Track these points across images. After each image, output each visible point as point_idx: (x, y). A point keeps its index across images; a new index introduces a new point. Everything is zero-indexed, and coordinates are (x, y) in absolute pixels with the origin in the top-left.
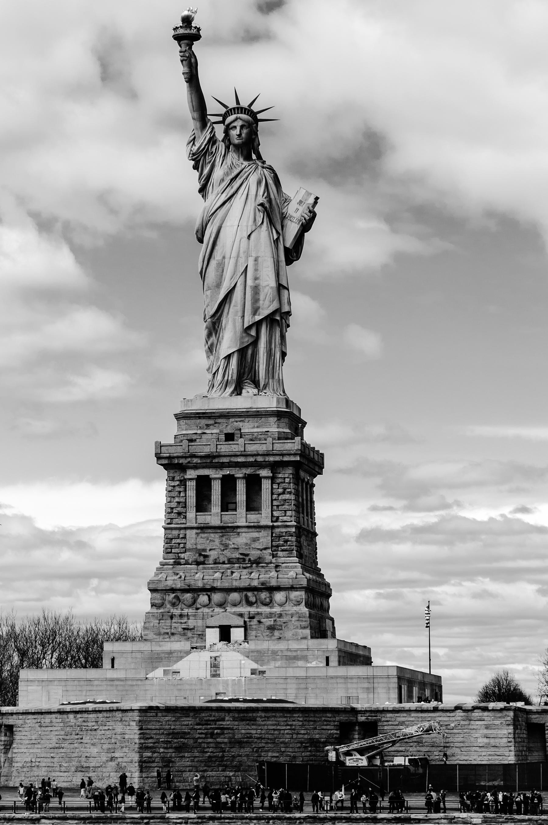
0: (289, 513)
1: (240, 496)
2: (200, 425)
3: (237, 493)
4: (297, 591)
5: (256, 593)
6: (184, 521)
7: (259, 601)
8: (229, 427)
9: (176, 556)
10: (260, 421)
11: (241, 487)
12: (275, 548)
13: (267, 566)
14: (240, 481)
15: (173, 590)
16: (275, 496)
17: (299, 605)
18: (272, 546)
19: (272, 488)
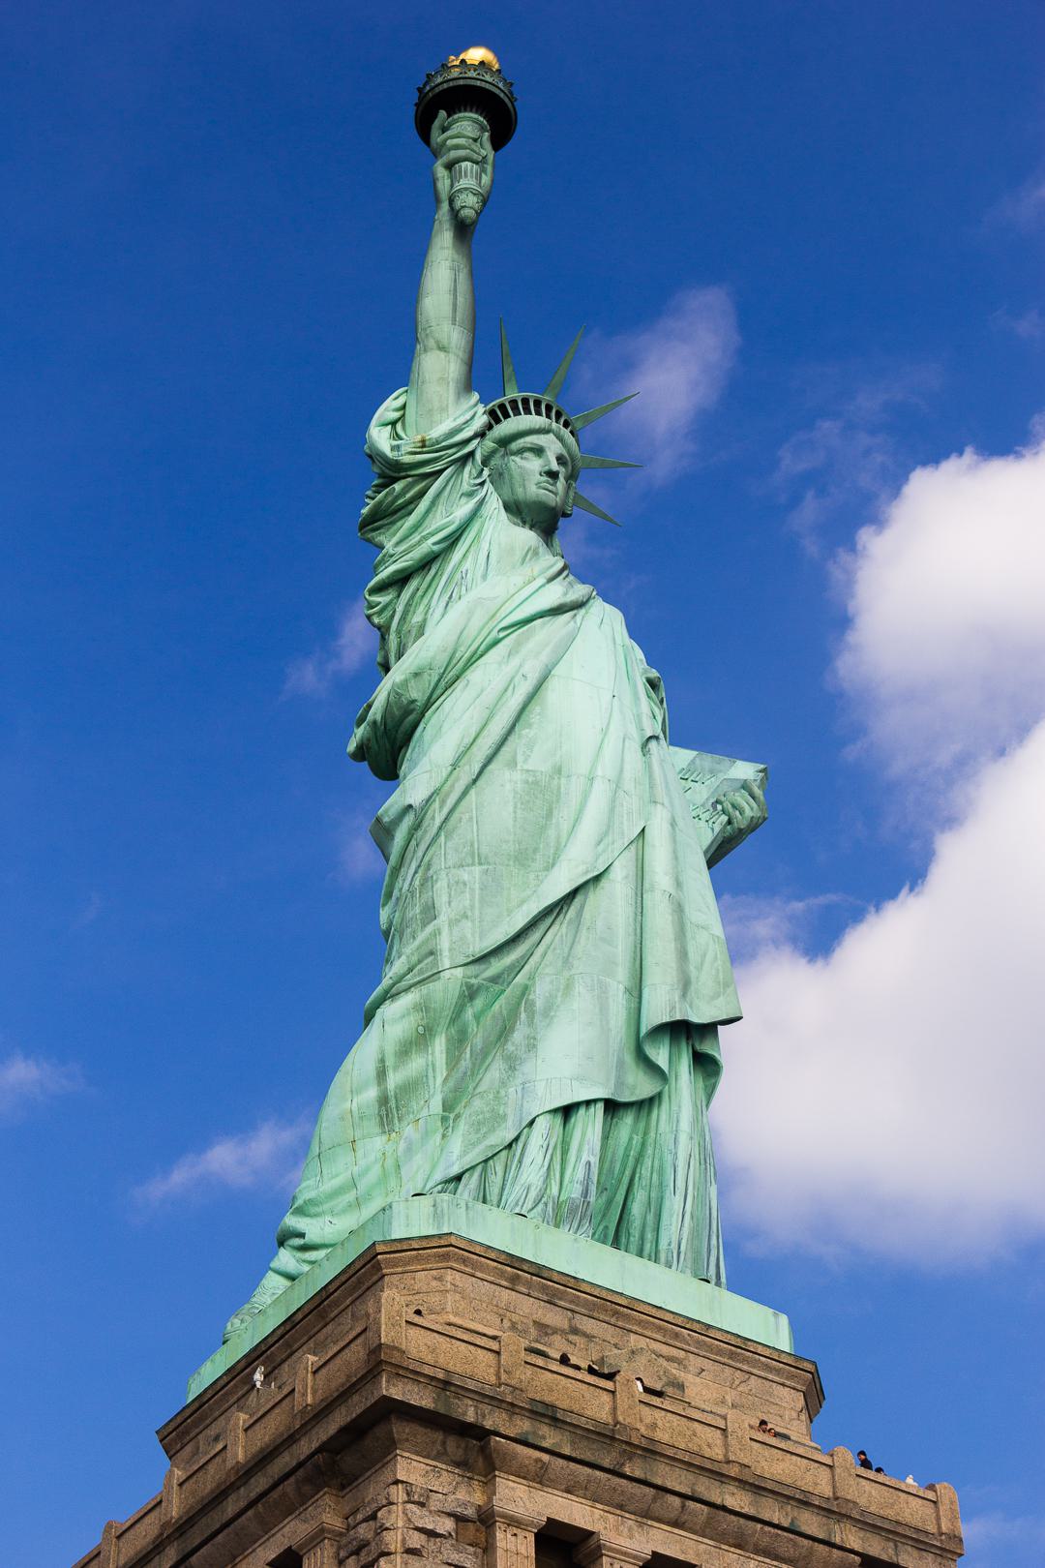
2: (515, 1318)
8: (642, 1360)
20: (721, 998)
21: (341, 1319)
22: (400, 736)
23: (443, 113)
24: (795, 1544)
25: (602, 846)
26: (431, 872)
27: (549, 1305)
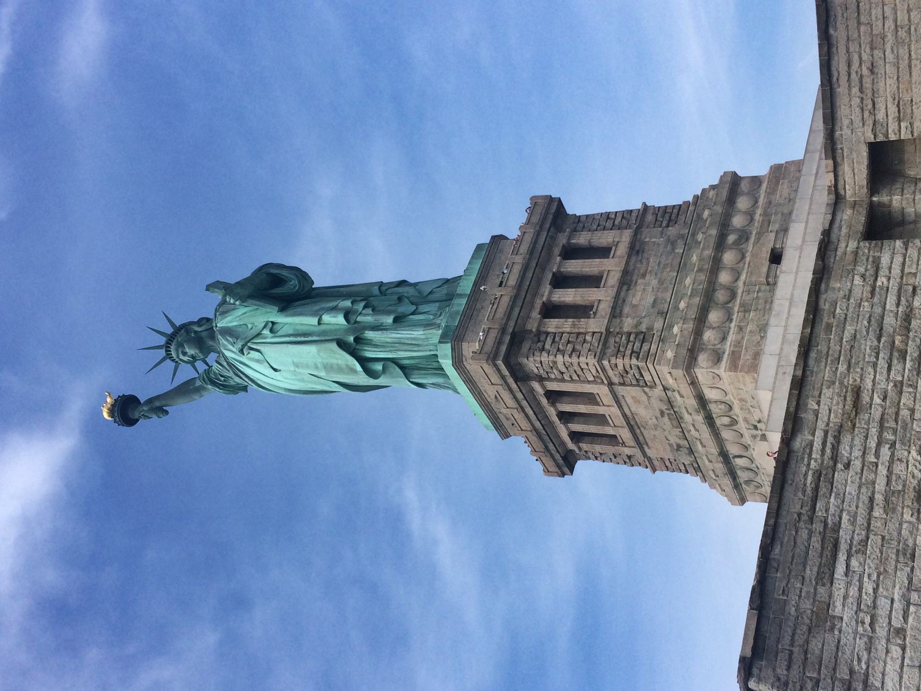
0: (584, 366)
4: (696, 377)
5: (714, 416)
12: (641, 383)
13: (671, 398)
15: (737, 486)
16: (567, 377)
17: (719, 376)
18: (638, 385)
19: (556, 380)
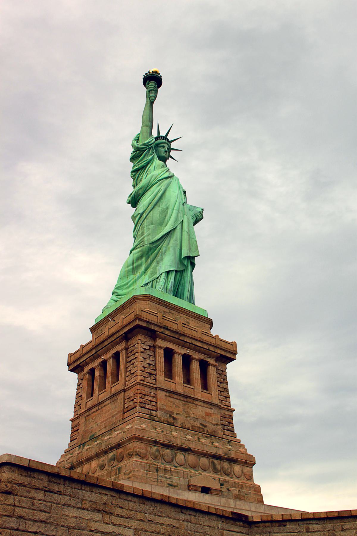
1: (196, 374)
2: (160, 310)
3: (194, 371)
6: (154, 382)
7: (222, 470)
8: (182, 318)
9: (149, 412)
10: (199, 324)
11: (195, 367)
12: (223, 426)
13: (222, 440)
14: (195, 362)
15: (155, 443)
18: (221, 424)
20: (196, 252)
21: (127, 309)
22: (137, 200)
23: (148, 81)
24: (209, 352)
25: (175, 223)
26: (143, 226)
27: (165, 308)
